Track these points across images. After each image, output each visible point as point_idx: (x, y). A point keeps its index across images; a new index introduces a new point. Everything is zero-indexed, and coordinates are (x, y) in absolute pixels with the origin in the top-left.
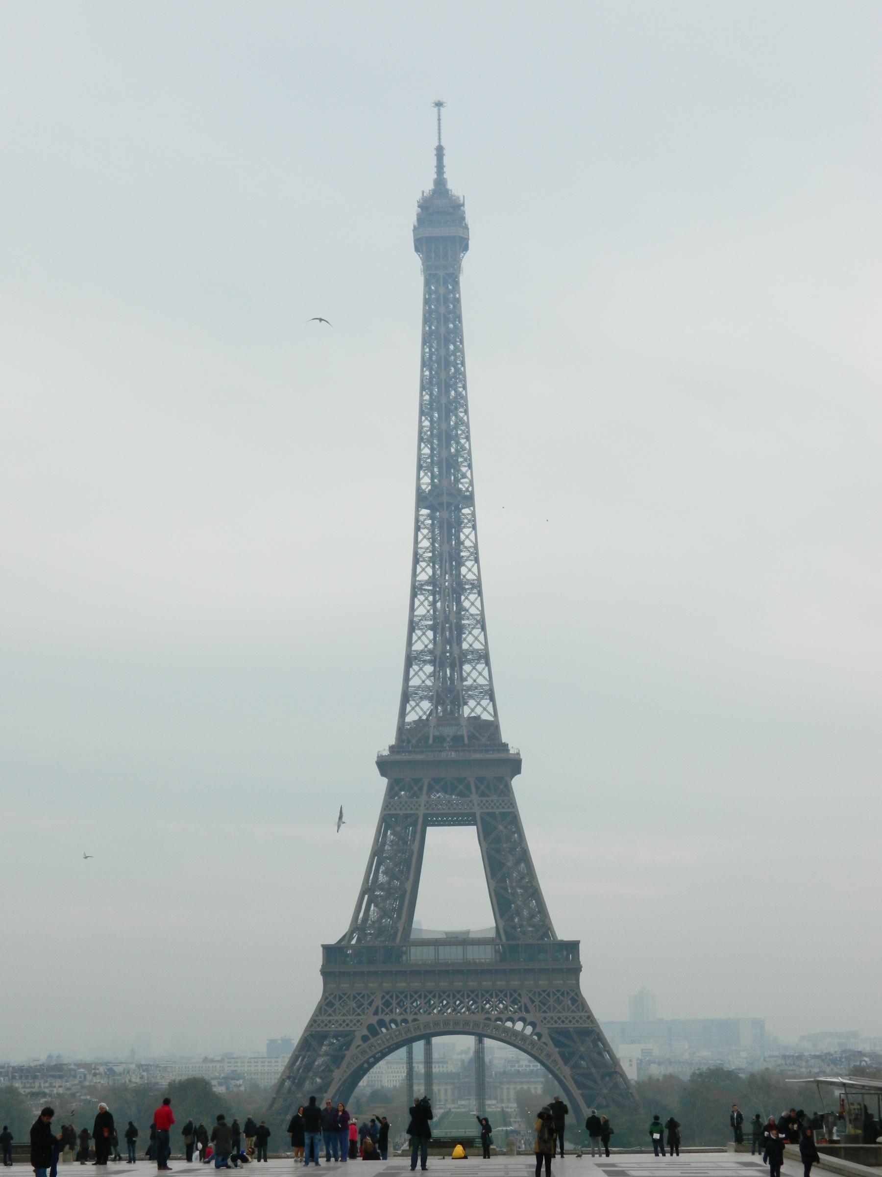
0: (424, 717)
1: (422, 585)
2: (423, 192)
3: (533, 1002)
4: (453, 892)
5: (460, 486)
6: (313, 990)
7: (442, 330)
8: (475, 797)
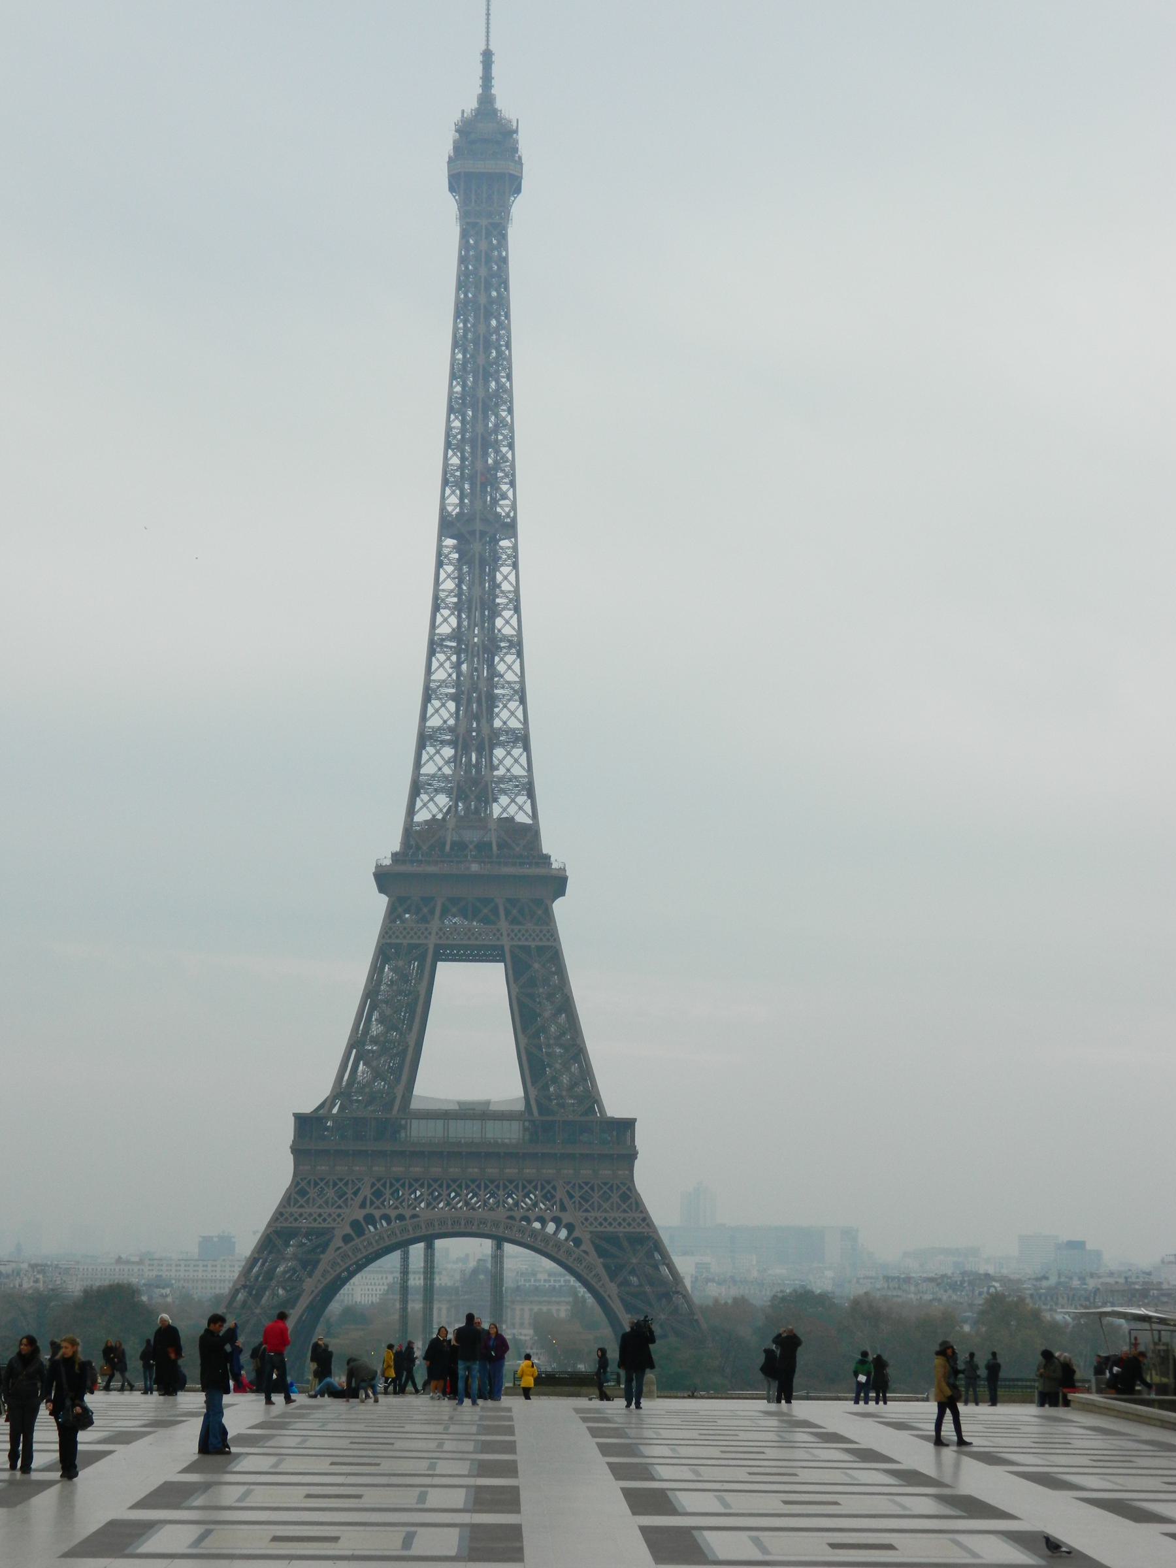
0: (440, 816)
1: (443, 640)
2: (463, 112)
3: (571, 1197)
4: (469, 1049)
5: (499, 510)
6: (276, 1172)
7: (483, 300)
8: (503, 925)
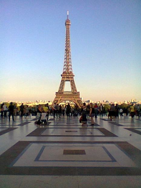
4: (68, 87)
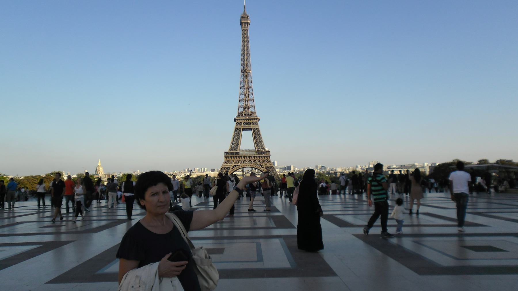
4: (247, 142)
6: (223, 159)
